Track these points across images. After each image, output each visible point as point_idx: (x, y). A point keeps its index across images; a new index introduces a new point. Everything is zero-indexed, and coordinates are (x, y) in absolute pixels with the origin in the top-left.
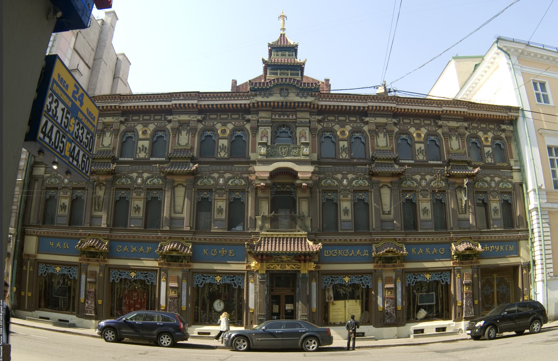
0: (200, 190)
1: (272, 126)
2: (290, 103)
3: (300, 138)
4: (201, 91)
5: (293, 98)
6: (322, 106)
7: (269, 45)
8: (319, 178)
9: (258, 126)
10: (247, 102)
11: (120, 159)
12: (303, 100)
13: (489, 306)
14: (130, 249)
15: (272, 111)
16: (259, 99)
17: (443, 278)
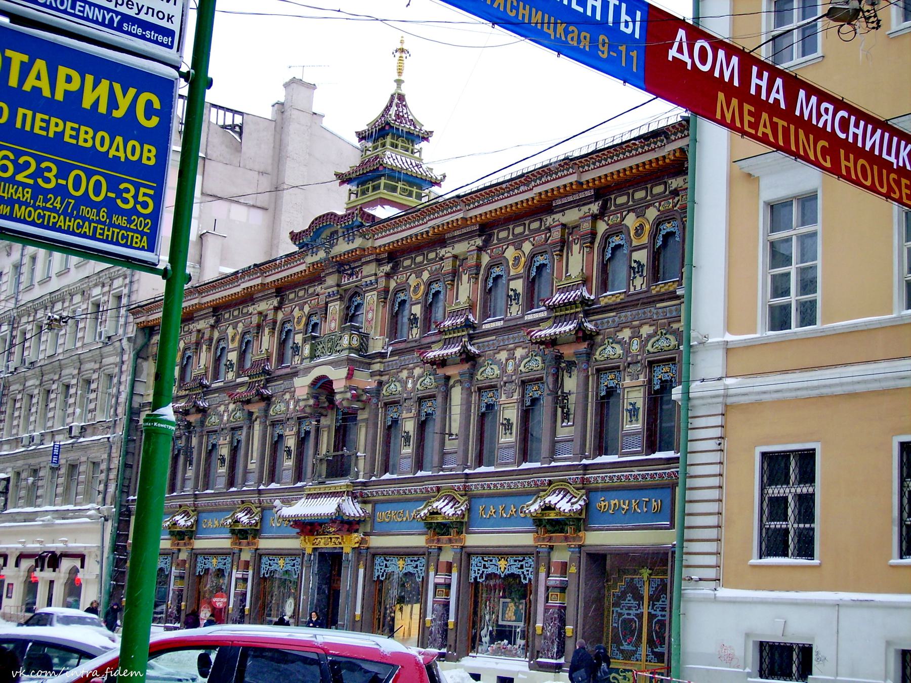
0: (274, 424)
1: (341, 299)
2: (340, 255)
3: (367, 312)
4: (258, 263)
5: (342, 247)
6: (380, 246)
7: (358, 134)
8: (380, 384)
9: (327, 304)
10: (302, 267)
11: (213, 386)
12: (352, 246)
13: (630, 648)
14: (213, 524)
15: (339, 272)
16: (310, 259)
17: (524, 570)
